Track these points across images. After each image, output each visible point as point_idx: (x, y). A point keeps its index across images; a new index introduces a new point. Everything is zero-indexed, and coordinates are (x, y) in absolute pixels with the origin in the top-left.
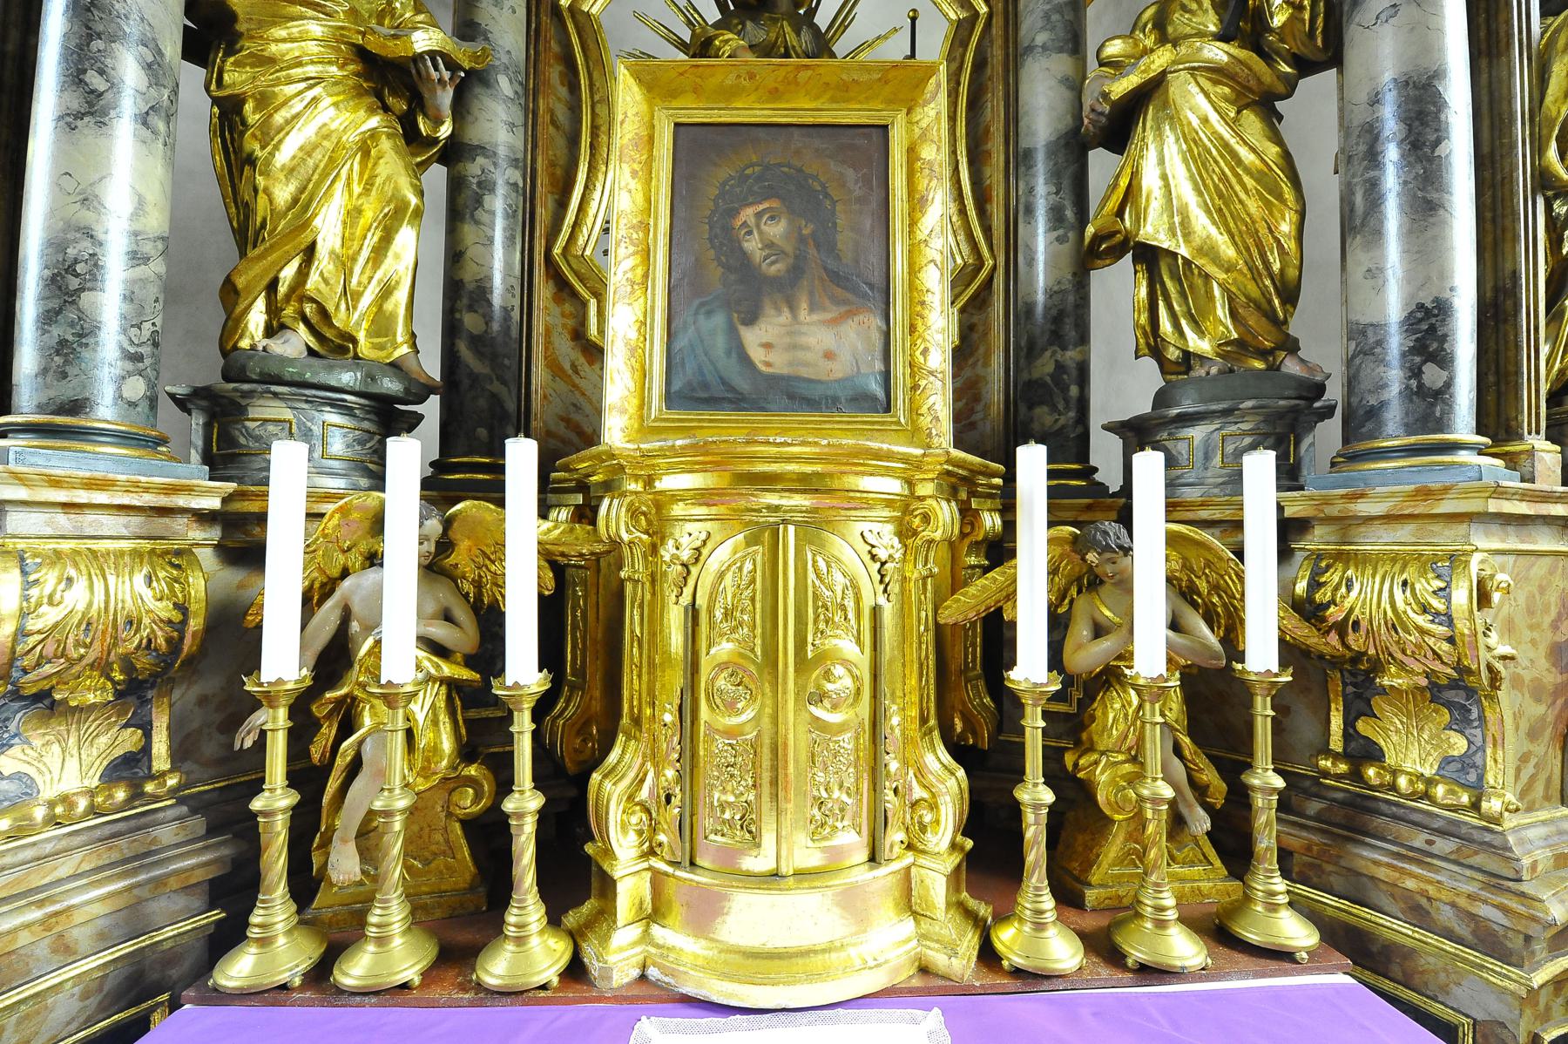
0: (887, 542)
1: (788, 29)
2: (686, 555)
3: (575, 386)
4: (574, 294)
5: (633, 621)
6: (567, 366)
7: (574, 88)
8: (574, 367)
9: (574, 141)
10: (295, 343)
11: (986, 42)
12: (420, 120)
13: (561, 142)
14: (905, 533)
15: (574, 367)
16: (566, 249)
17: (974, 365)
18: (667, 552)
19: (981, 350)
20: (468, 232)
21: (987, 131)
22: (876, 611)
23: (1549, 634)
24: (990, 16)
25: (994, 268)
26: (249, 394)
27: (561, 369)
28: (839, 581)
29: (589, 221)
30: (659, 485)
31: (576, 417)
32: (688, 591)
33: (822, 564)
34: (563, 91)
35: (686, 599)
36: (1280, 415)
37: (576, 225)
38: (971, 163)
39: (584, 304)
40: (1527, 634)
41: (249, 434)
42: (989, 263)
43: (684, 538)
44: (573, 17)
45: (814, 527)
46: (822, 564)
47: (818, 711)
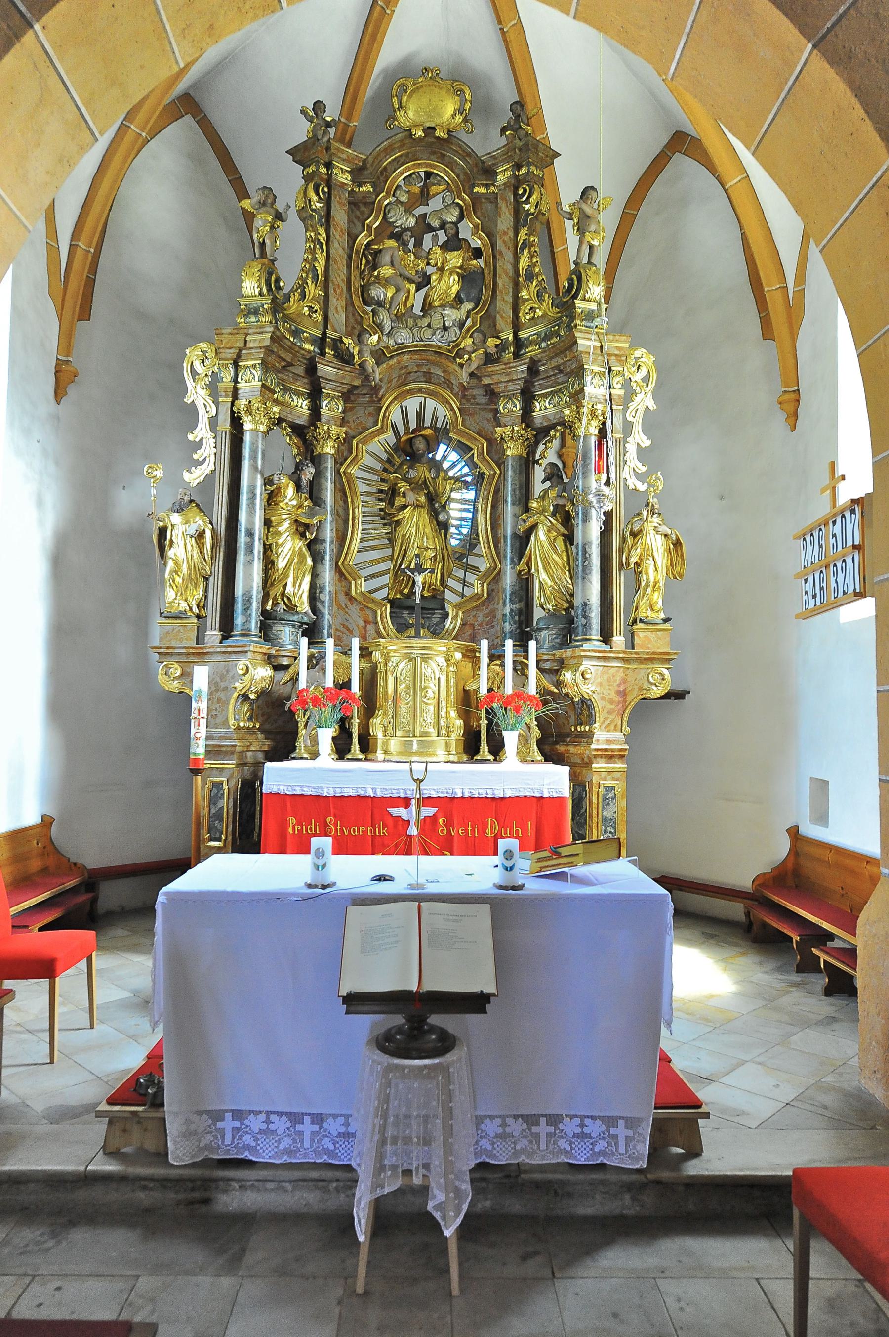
0: (441, 660)
1: (426, 471)
2: (394, 664)
4: (346, 578)
5: (381, 682)
6: (343, 605)
7: (346, 502)
8: (346, 605)
9: (346, 521)
10: (282, 607)
12: (307, 533)
13: (341, 522)
14: (447, 660)
16: (343, 562)
17: (494, 604)
18: (390, 664)
19: (496, 598)
20: (319, 566)
22: (439, 678)
23: (616, 688)
24: (501, 473)
26: (275, 623)
28: (429, 670)
29: (351, 552)
30: (388, 648)
31: (346, 624)
32: (395, 673)
33: (426, 666)
34: (341, 503)
35: (394, 675)
39: (350, 583)
40: (608, 687)
41: (273, 634)
42: (499, 566)
43: (394, 660)
45: (425, 659)
46: (426, 666)
47: (424, 700)
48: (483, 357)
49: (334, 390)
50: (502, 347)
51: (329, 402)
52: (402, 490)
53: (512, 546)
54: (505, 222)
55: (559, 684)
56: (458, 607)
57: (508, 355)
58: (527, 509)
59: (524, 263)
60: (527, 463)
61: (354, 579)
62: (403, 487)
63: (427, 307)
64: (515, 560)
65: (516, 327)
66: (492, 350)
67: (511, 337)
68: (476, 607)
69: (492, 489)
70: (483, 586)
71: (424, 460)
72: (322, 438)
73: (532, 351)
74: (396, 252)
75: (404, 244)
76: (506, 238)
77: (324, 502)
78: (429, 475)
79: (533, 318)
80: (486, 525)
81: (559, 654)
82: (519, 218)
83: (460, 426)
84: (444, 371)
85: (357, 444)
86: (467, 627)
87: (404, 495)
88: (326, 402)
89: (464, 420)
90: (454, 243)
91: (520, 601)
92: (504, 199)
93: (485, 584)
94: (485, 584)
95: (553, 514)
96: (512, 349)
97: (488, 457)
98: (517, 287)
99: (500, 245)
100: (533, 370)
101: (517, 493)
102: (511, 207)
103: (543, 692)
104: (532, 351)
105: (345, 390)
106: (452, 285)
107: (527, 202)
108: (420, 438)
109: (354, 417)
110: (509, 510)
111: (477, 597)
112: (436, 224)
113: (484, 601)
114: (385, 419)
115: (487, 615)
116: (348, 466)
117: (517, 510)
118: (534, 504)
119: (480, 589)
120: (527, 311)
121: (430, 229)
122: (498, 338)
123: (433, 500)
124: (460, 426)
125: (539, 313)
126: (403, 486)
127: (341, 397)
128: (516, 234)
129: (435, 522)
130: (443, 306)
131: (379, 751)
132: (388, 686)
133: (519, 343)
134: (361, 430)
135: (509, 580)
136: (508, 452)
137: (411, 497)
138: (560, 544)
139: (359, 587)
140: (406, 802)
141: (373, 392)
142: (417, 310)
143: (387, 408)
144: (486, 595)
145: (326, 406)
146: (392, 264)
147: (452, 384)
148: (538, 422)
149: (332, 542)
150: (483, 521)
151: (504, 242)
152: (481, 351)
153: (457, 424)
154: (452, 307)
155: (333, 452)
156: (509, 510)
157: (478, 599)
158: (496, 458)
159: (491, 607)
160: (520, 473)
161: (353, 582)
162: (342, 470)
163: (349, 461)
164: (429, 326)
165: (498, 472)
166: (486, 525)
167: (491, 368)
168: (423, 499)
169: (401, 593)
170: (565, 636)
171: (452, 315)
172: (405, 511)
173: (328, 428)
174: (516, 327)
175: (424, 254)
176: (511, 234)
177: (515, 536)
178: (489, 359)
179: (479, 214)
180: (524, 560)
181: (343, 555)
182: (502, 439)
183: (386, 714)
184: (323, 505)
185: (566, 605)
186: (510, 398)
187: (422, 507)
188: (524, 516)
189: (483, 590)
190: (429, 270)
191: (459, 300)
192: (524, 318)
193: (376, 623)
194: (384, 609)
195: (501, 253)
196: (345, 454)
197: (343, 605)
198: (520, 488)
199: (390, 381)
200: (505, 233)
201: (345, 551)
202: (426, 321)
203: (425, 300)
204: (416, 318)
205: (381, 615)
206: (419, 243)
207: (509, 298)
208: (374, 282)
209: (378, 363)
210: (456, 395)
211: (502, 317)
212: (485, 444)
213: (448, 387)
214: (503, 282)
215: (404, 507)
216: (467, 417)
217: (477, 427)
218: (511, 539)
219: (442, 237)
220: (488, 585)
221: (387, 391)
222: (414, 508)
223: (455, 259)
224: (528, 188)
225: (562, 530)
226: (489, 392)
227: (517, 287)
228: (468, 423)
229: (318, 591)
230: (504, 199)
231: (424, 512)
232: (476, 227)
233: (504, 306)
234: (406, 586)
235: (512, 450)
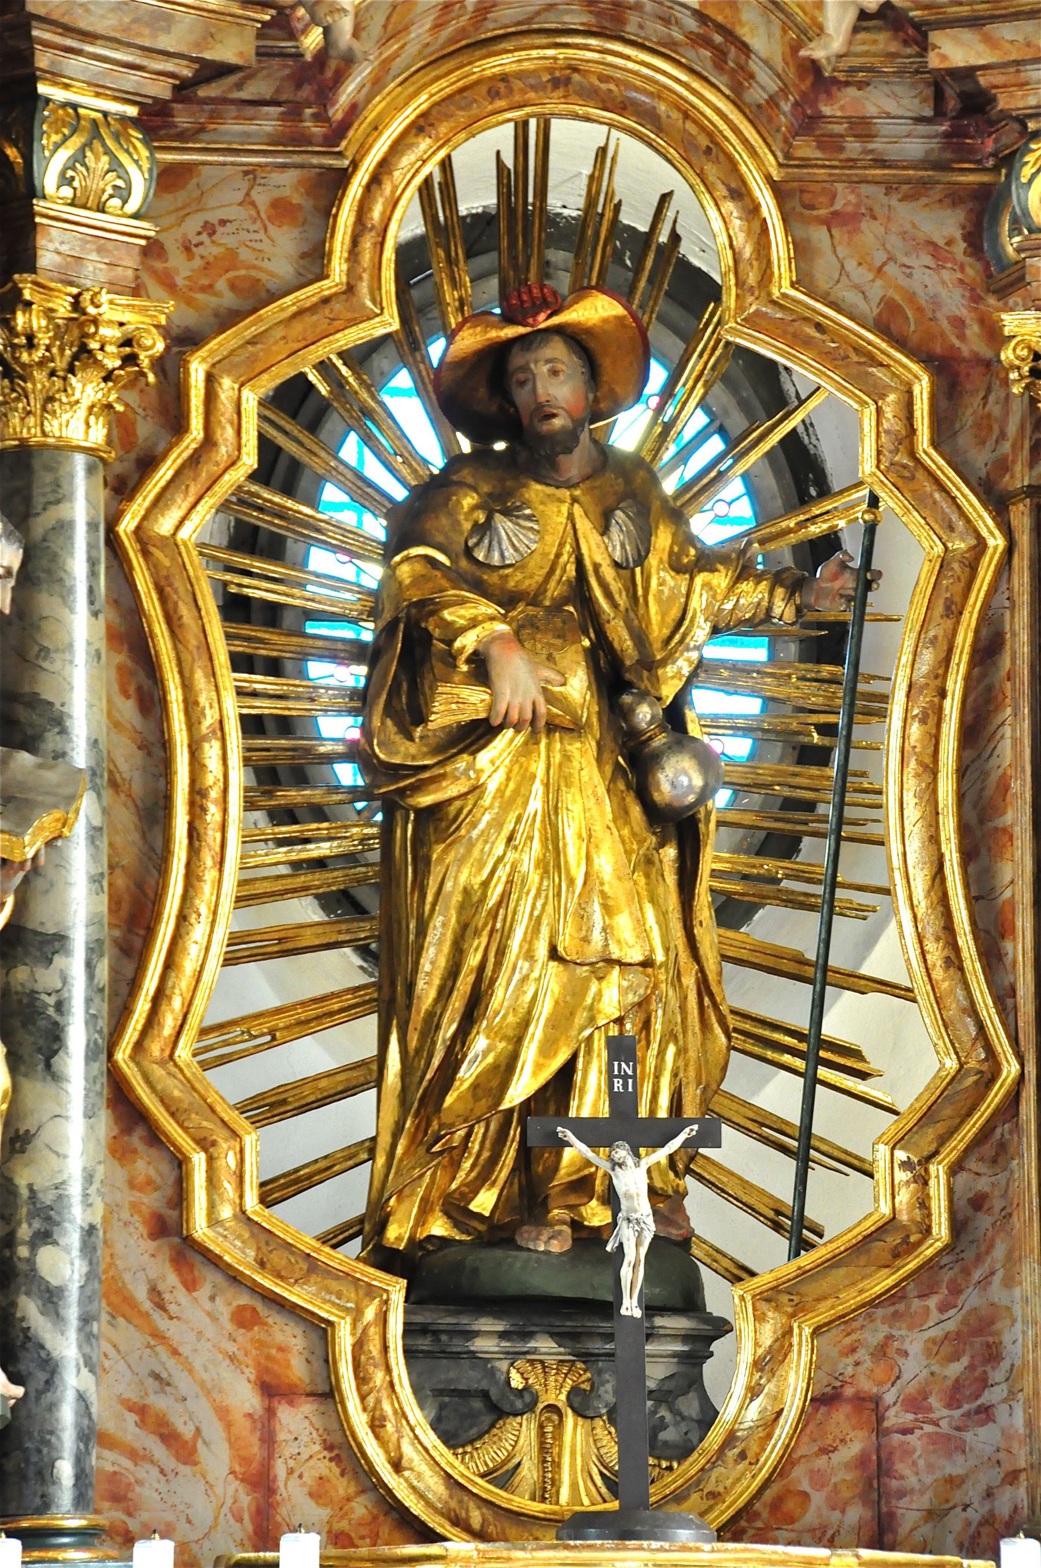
1: (584, 526)
3: (158, 1336)
4: (155, 1137)
6: (141, 1293)
8: (155, 1294)
11: (1001, 599)
15: (155, 1294)
16: (139, 1046)
17: (985, 1281)
19: (999, 1252)
21: (1004, 787)
25: (1021, 1078)
27: (129, 1301)
31: (160, 1403)
37: (160, 996)
38: (968, 855)
39: (180, 1163)
42: (1010, 1069)
44: (146, 553)
49: (99, 90)
51: (79, 157)
52: (467, 642)
61: (205, 1144)
68: (894, 1296)
69: (964, 639)
70: (923, 1181)
71: (574, 464)
72: (42, 363)
77: (59, 722)
80: (934, 839)
83: (783, 284)
85: (211, 380)
86: (840, 1417)
88: (63, 155)
89: (801, 251)
93: (938, 1170)
94: (938, 1170)
97: (934, 461)
105: (162, 89)
108: (557, 350)
109: (193, 225)
111: (893, 1240)
113: (930, 1266)
114: (367, 244)
116: (160, 502)
119: (904, 1197)
123: (627, 686)
124: (783, 284)
126: (474, 623)
127: (135, 122)
129: (636, 811)
134: (228, 299)
139: (229, 1188)
141: (306, 92)
143: (376, 180)
144: (941, 1230)
145: (65, 180)
147: (745, 49)
149: (94, 950)
150: (913, 813)
153: (766, 276)
155: (98, 434)
157: (898, 1254)
158: (981, 459)
159: (971, 1299)
161: (198, 1160)
162: (127, 526)
163: (165, 473)
165: (996, 542)
166: (934, 839)
172: (484, 758)
173: (76, 305)
181: (142, 1006)
184: (51, 740)
187: (574, 729)
189: (923, 1203)
194: (370, 1313)
196: (145, 429)
197: (141, 1293)
199: (393, 32)
201: (150, 984)
205: (359, 1346)
210: (755, 115)
212: (922, 388)
213: (720, 56)
216: (819, 235)
217: (877, 290)
220: (955, 1169)
221: (377, 83)
222: (534, 738)
226: (952, 104)
228: (824, 270)
229: (24, 1232)
234: (483, 1177)
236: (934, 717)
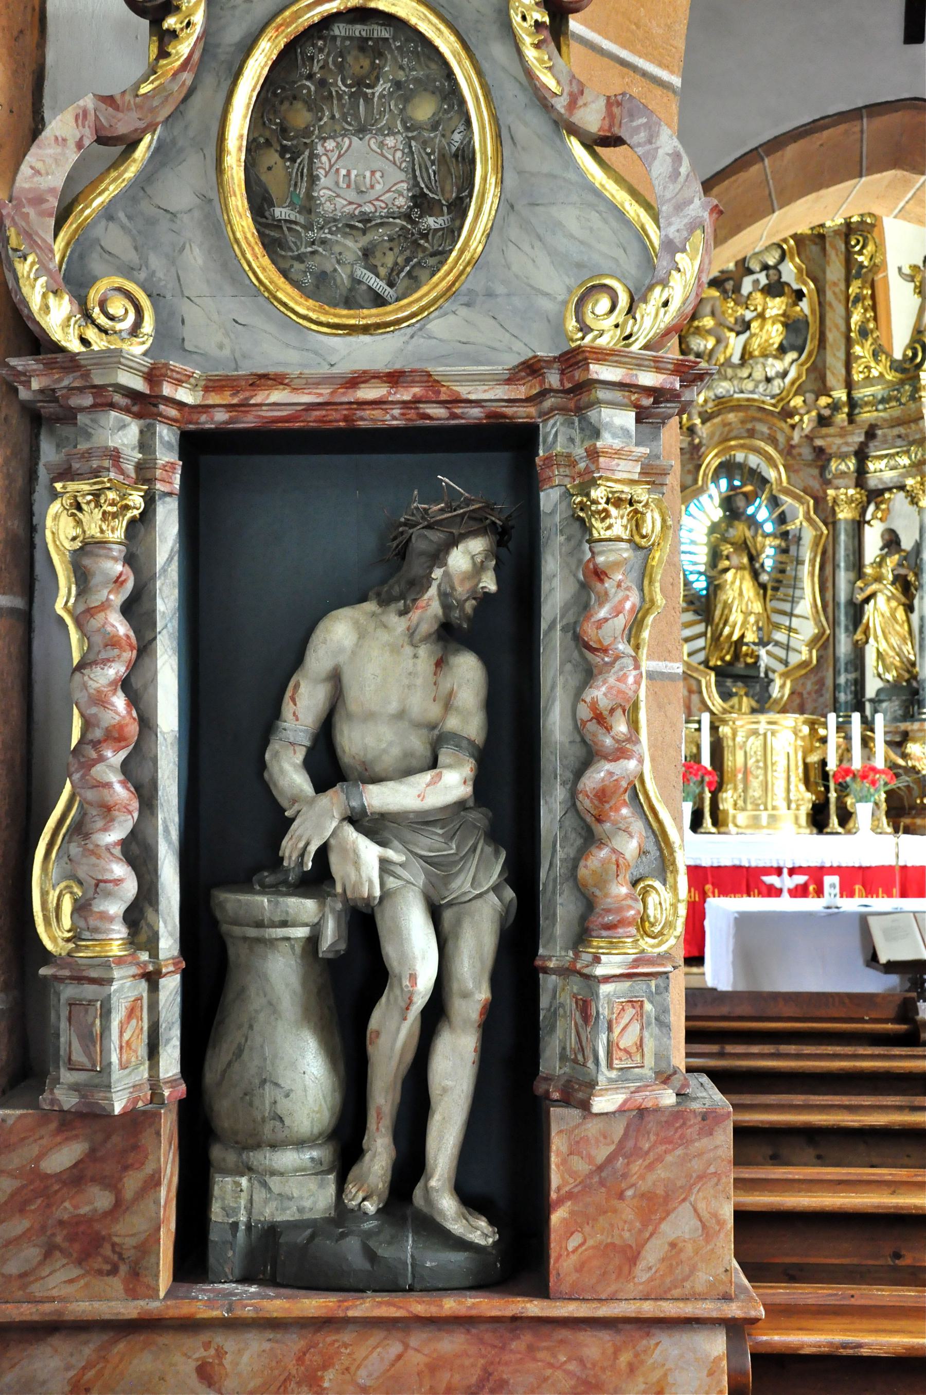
36: (905, 701)
42: (828, 632)
48: (816, 419)
50: (835, 407)
52: (725, 553)
53: (846, 614)
54: (835, 271)
55: (905, 756)
56: (785, 675)
57: (841, 417)
58: (860, 575)
59: (856, 318)
60: (859, 525)
62: (727, 549)
63: (746, 355)
64: (851, 628)
65: (849, 385)
66: (827, 412)
67: (844, 398)
68: (806, 674)
71: (744, 518)
73: (867, 416)
74: (718, 303)
75: (724, 292)
76: (837, 290)
78: (749, 534)
79: (868, 377)
81: (903, 726)
82: (852, 270)
83: (785, 484)
84: (770, 428)
86: (795, 696)
87: (728, 558)
89: (788, 478)
90: (775, 289)
91: (856, 670)
92: (834, 247)
95: (893, 583)
96: (846, 410)
97: (814, 517)
98: (849, 343)
99: (829, 296)
100: (871, 434)
101: (851, 558)
102: (842, 257)
103: (893, 766)
104: (867, 416)
106: (775, 334)
107: (860, 253)
108: (741, 496)
110: (843, 577)
112: (755, 266)
115: (816, 683)
117: (852, 575)
118: (868, 570)
120: (861, 369)
121: (750, 272)
122: (830, 396)
125: (875, 373)
128: (848, 287)
130: (765, 356)
131: (731, 825)
132: (734, 760)
133: (852, 403)
135: (844, 647)
136: (841, 516)
137: (735, 560)
138: (900, 614)
140: (778, 871)
142: (736, 359)
144: (815, 661)
146: (713, 314)
148: (873, 482)
151: (834, 293)
152: (814, 413)
154: (775, 357)
156: (843, 577)
158: (823, 517)
159: (820, 674)
160: (853, 537)
164: (750, 376)
165: (826, 532)
167: (824, 431)
168: (745, 560)
169: (722, 659)
170: (907, 708)
171: (774, 366)
174: (849, 385)
175: (744, 300)
176: (842, 286)
177: (851, 603)
178: (823, 421)
179: (803, 257)
180: (860, 629)
182: (835, 501)
183: (735, 789)
185: (907, 676)
186: (843, 457)
188: (859, 584)
190: (749, 315)
191: (782, 350)
192: (857, 377)
193: (700, 692)
195: (830, 305)
198: (854, 554)
200: (835, 284)
202: (745, 373)
203: (744, 348)
204: (733, 366)
206: (737, 289)
207: (842, 355)
208: (694, 334)
209: (703, 423)
211: (833, 374)
212: (812, 502)
214: (834, 336)
215: (726, 570)
218: (846, 607)
219: (763, 280)
223: (776, 306)
224: (861, 239)
225: (903, 599)
227: (849, 343)
230: (834, 247)
231: (747, 575)
232: (800, 270)
233: (835, 361)
234: (728, 653)
235: (845, 514)
236: (813, 566)
